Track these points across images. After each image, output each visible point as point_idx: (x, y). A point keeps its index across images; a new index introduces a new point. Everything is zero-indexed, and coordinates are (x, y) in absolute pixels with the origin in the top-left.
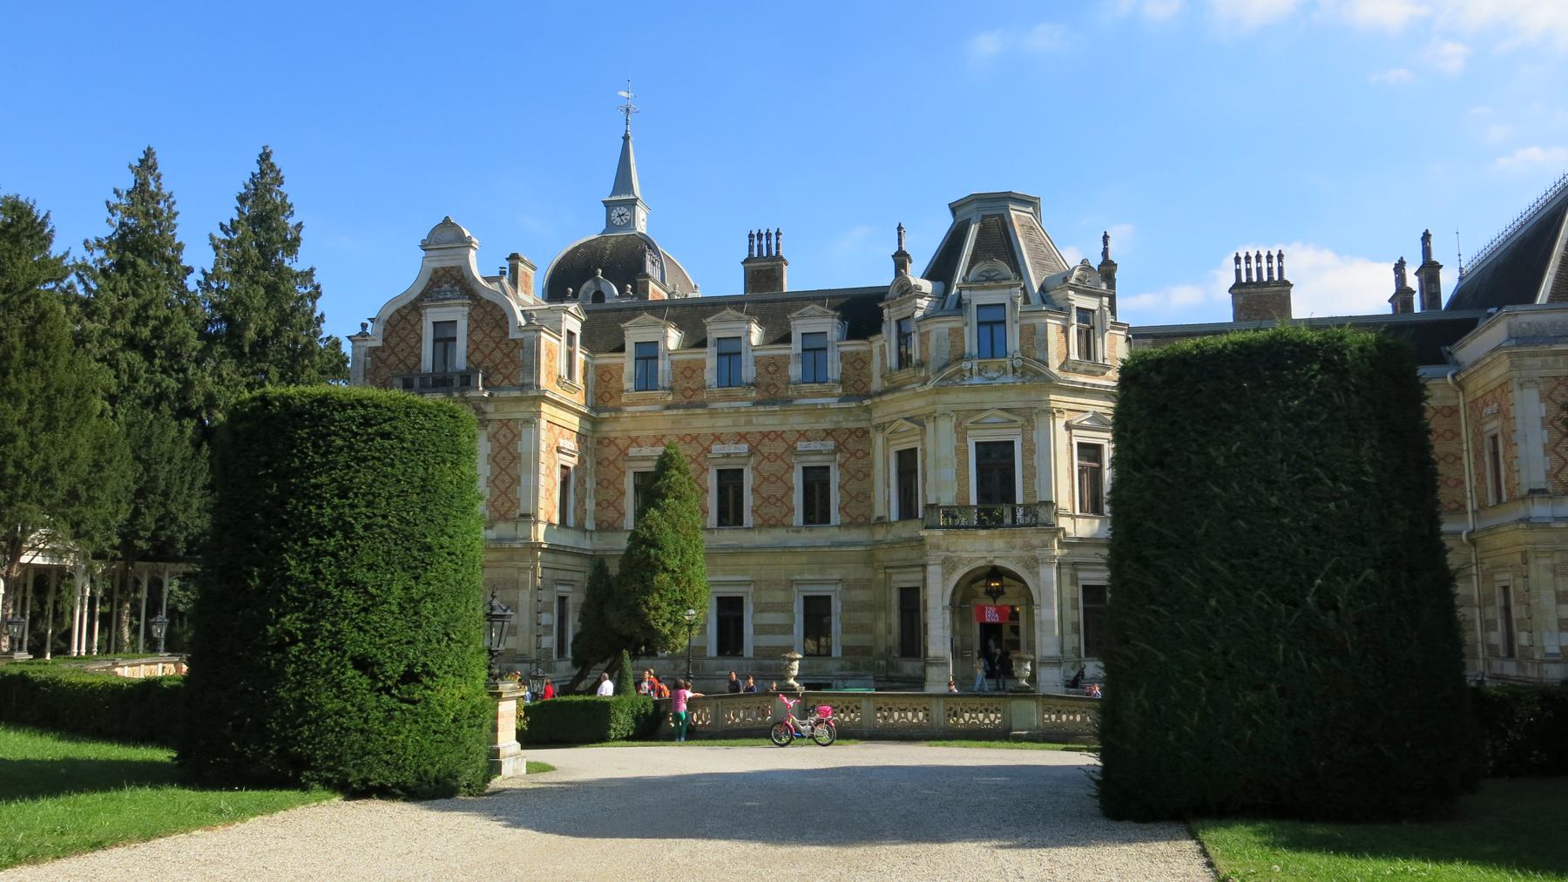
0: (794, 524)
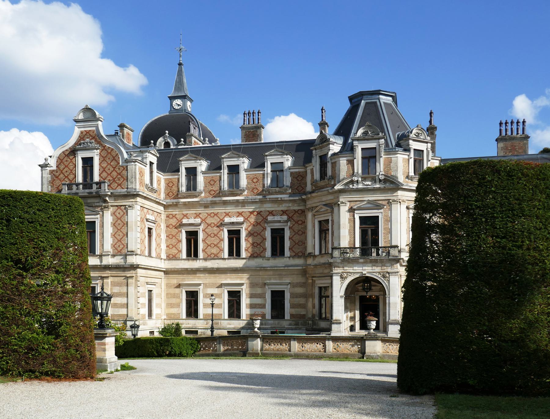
0: (266, 256)
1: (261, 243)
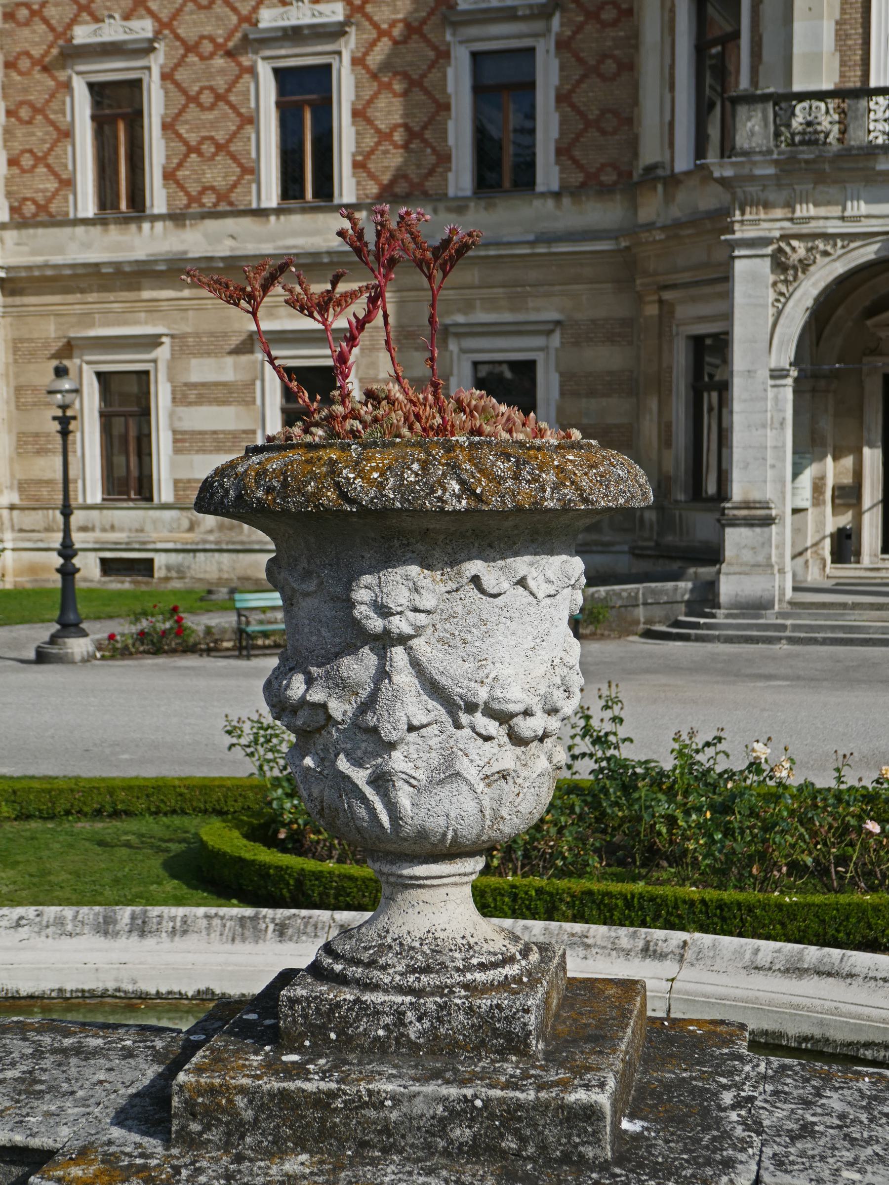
0: (451, 192)
1: (425, 127)
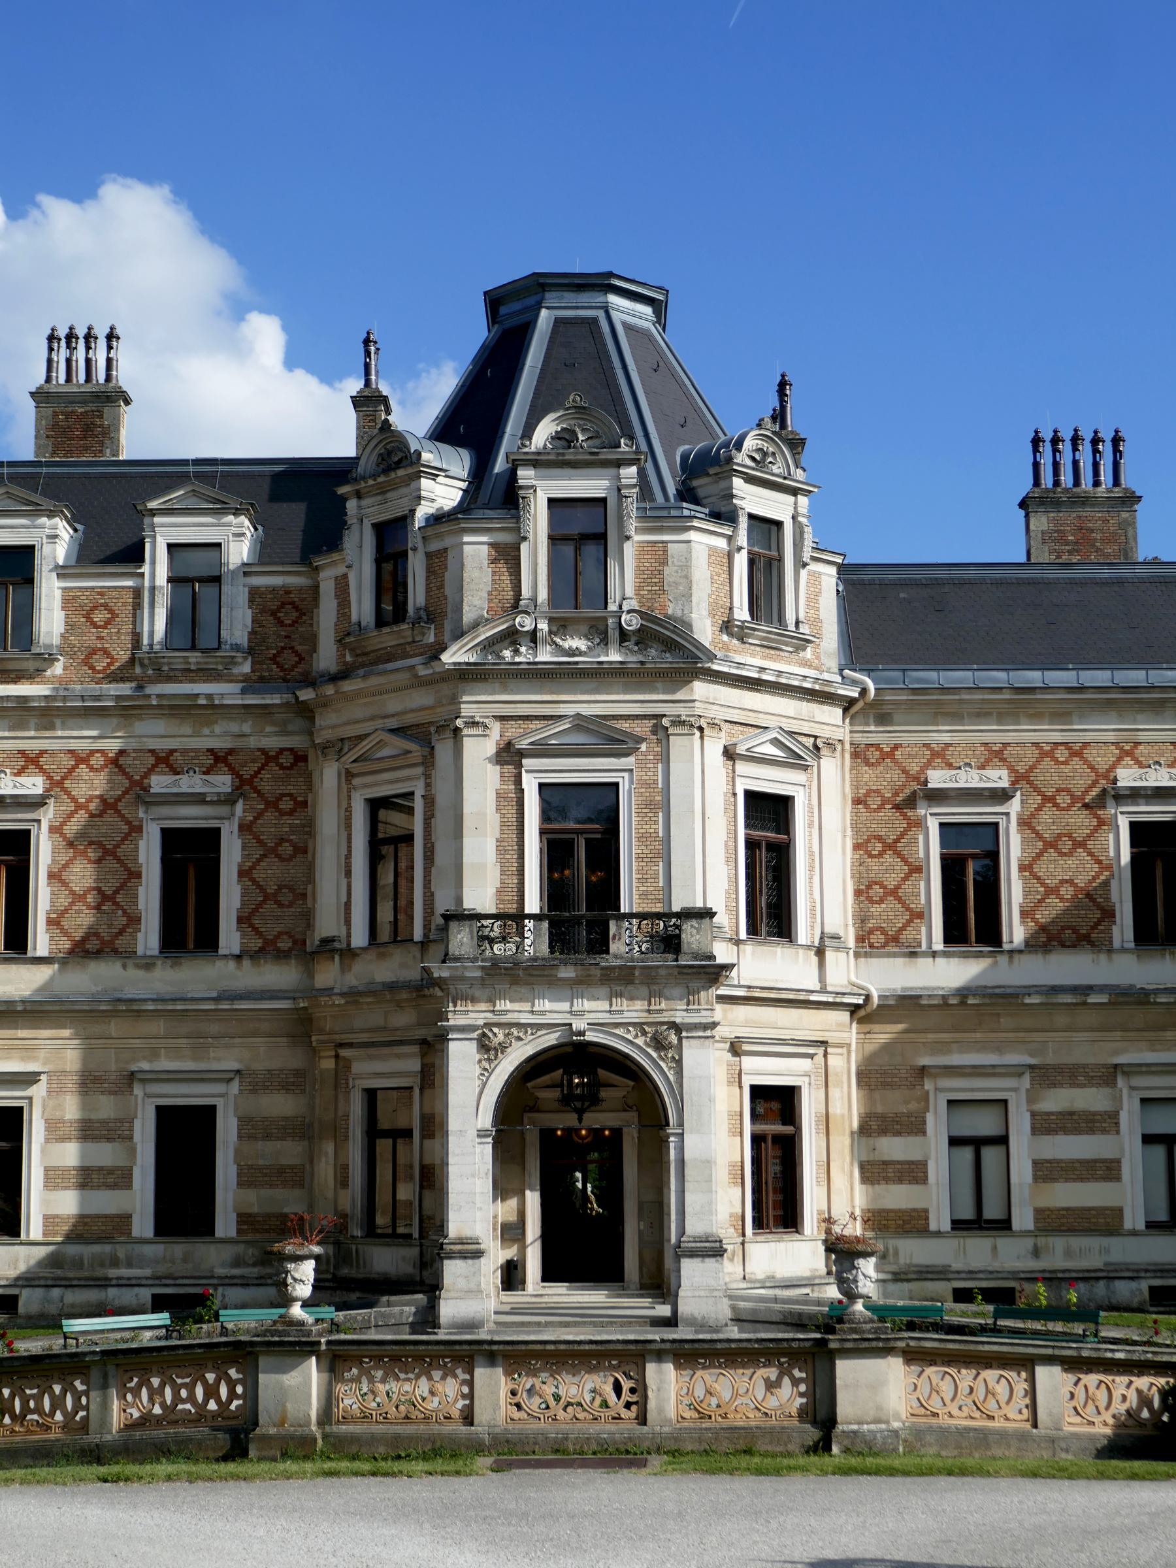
0: (140, 951)
1: (117, 892)
